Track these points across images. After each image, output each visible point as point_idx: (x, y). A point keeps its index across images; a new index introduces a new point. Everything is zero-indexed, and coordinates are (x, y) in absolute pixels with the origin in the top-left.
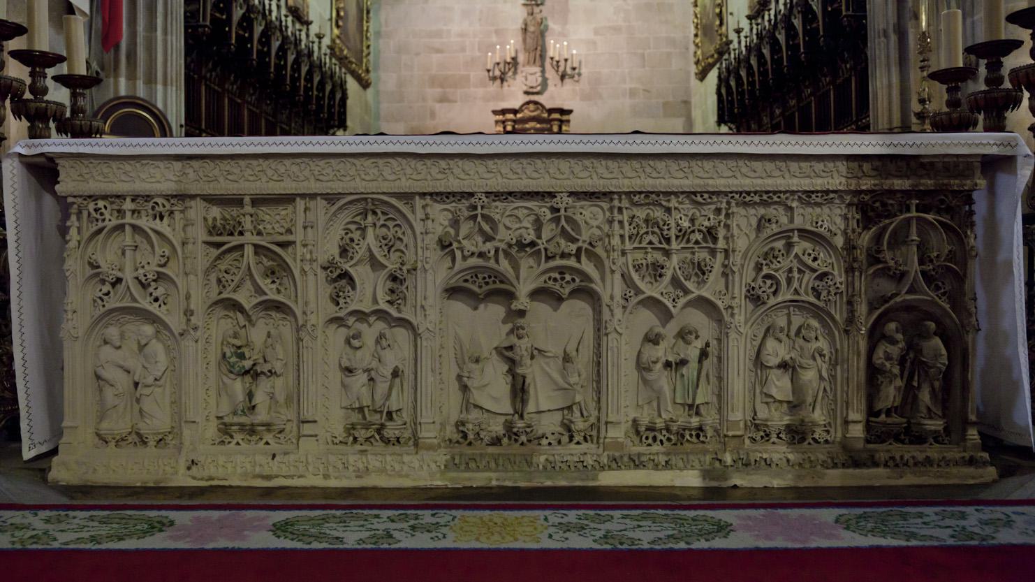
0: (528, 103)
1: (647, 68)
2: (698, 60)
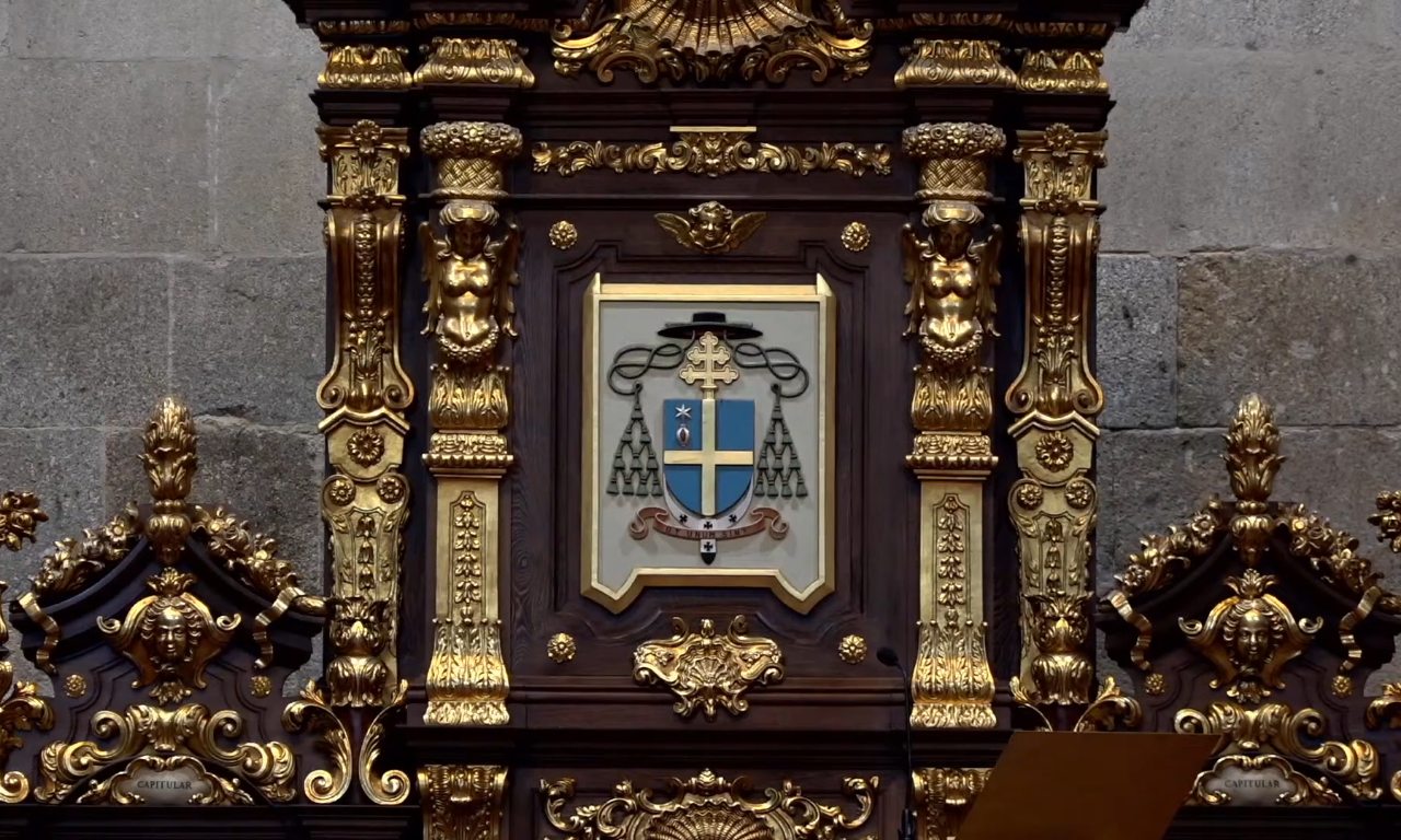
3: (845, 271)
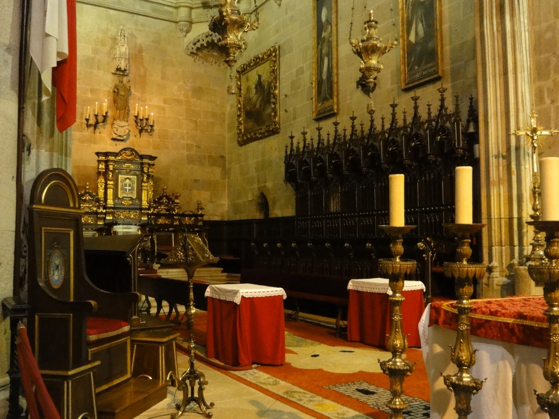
0: (125, 149)
1: (198, 131)
2: (240, 133)
3: (137, 175)
